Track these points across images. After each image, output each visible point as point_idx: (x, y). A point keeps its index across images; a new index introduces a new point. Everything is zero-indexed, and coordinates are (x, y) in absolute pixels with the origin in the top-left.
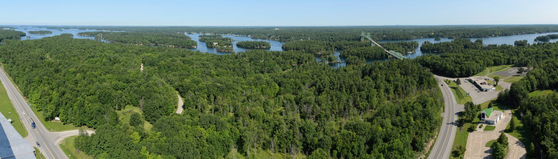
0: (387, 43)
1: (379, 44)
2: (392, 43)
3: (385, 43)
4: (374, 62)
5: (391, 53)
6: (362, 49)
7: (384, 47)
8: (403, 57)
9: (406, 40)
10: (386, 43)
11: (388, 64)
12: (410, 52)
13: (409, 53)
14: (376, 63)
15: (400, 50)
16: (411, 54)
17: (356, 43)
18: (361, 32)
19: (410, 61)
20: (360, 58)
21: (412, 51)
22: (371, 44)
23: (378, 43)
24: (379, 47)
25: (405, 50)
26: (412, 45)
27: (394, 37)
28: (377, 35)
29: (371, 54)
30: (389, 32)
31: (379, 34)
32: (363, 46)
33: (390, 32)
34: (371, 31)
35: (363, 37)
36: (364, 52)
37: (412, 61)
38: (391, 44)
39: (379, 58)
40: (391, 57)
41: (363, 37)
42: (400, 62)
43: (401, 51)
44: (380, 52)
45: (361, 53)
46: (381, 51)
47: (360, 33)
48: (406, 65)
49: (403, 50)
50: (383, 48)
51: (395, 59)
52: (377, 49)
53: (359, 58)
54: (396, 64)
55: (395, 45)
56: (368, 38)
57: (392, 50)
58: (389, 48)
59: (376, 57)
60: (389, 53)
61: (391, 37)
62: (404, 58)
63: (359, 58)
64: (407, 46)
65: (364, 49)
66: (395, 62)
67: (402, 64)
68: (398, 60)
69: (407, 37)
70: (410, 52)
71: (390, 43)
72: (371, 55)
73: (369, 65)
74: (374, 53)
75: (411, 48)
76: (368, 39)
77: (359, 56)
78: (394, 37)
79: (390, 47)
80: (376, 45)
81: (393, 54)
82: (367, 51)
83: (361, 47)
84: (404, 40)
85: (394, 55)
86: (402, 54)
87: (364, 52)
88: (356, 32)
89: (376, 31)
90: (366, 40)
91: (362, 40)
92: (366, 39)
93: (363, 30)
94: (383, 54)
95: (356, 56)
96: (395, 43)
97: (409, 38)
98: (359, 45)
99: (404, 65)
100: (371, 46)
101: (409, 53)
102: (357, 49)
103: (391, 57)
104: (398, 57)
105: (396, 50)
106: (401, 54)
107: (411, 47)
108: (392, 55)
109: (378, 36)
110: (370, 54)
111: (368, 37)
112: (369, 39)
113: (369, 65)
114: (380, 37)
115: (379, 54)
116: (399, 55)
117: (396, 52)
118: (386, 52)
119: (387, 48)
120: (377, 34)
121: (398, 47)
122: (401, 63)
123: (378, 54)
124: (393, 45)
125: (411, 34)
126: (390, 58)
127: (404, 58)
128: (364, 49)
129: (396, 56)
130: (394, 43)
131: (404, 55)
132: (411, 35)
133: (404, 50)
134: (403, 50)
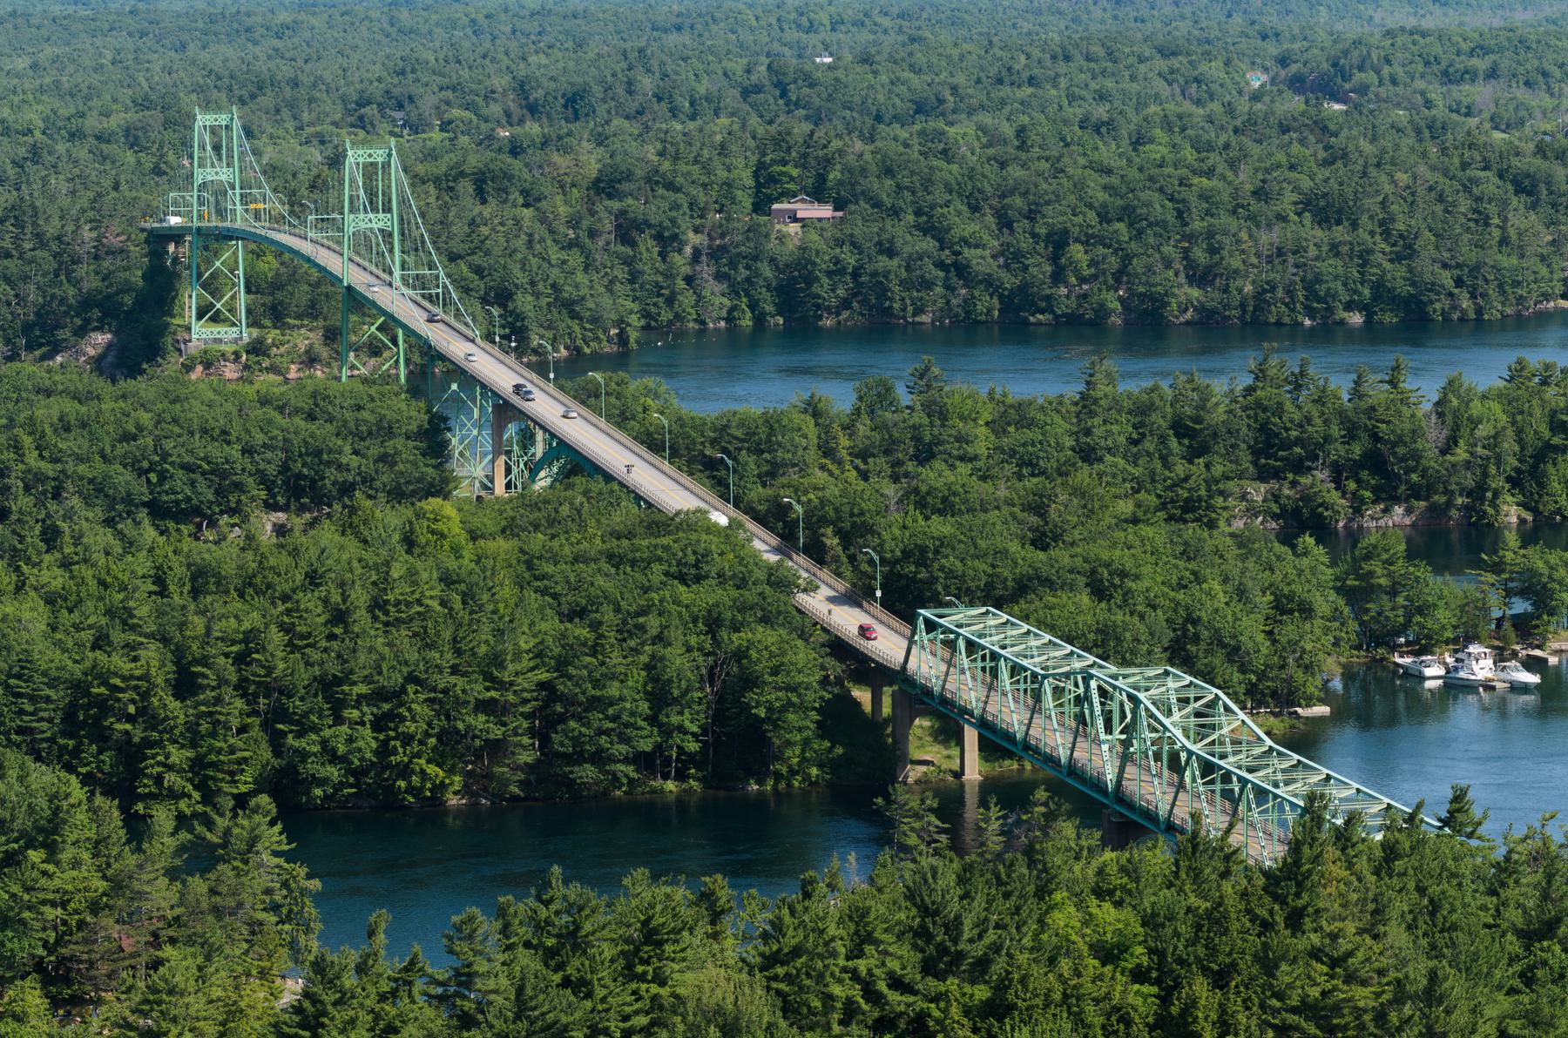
0: (877, 399)
1: (652, 443)
2: (1014, 416)
3: (814, 409)
4: (522, 908)
5: (968, 690)
6: (201, 580)
7: (774, 518)
8: (1293, 793)
9: (1372, 335)
10: (840, 398)
11: (903, 958)
12: (1482, 667)
13: (1455, 687)
14: (573, 939)
15: (1214, 599)
16: (1499, 702)
17: (47, 411)
18: (183, 123)
19: (1471, 904)
20: (163, 817)
21: (1525, 628)
22: (434, 440)
23: (621, 419)
24: (657, 521)
25: (1357, 594)
26: (1529, 480)
27: (1058, 242)
28: (606, 186)
29: (444, 704)
30: (920, 108)
31: (655, 180)
32: (226, 485)
33: (962, 132)
34: (428, 102)
35: (234, 260)
36: (247, 648)
37: (1524, 891)
38: (983, 440)
39: (652, 814)
40: (974, 769)
41: (234, 260)
42: (1214, 920)
43: (1251, 630)
44: (681, 662)
45: (185, 685)
46: (713, 624)
47: (133, 137)
48: (1363, 996)
49: (1287, 606)
50: (763, 545)
51: (1067, 829)
52: (605, 582)
53: (137, 828)
54: (1108, 954)
55: (1088, 454)
56: (355, 277)
57: (997, 596)
58: (918, 554)
59: (587, 773)
60: (926, 666)
61: (981, 260)
62: (1313, 807)
63: (137, 828)
64: (1388, 495)
65: (249, 586)
66: (1065, 918)
67: (1268, 965)
68: (1157, 857)
69: (1405, 251)
70: (1482, 667)
71: (937, 412)
72: (450, 744)
73: (402, 983)
74: (525, 677)
75: (1511, 548)
76: (356, 301)
77: (132, 756)
78: (1058, 242)
79: (941, 527)
80: (576, 465)
81: (1011, 714)
82: (340, 616)
83: (159, 512)
84: (1327, 333)
85: (1055, 738)
86: (1255, 697)
87: (247, 648)
88: (33, 116)
89: (575, 104)
90: (306, 338)
91: (201, 333)
92: (312, 311)
93: (225, 54)
94: (760, 702)
95: (43, 777)
96: (1086, 403)
97: (1472, 276)
98: (123, 478)
99: (1310, 982)
100: (441, 488)
101: (1455, 687)
102: (53, 577)
103: (974, 769)
104: (1152, 790)
105: (1099, 591)
106: (1236, 720)
107: (1511, 513)
108: (996, 743)
109: (627, 230)
110: (419, 714)
111: (363, 243)
112: (398, 301)
113: (402, 983)
114: (668, 241)
115: (660, 696)
116: (1175, 723)
117: (1106, 644)
118: (839, 647)
119: (855, 532)
120: (591, 161)
121: (1157, 532)
122: (1240, 940)
123: (629, 693)
124: (1028, 464)
125: (1525, 186)
126: (949, 803)
127: (1313, 807)
128: (249, 586)
129: (1102, 760)
130: (1061, 428)
131: (1304, 741)
132: (1521, 218)
133: (1324, 602)
134: (1287, 606)
